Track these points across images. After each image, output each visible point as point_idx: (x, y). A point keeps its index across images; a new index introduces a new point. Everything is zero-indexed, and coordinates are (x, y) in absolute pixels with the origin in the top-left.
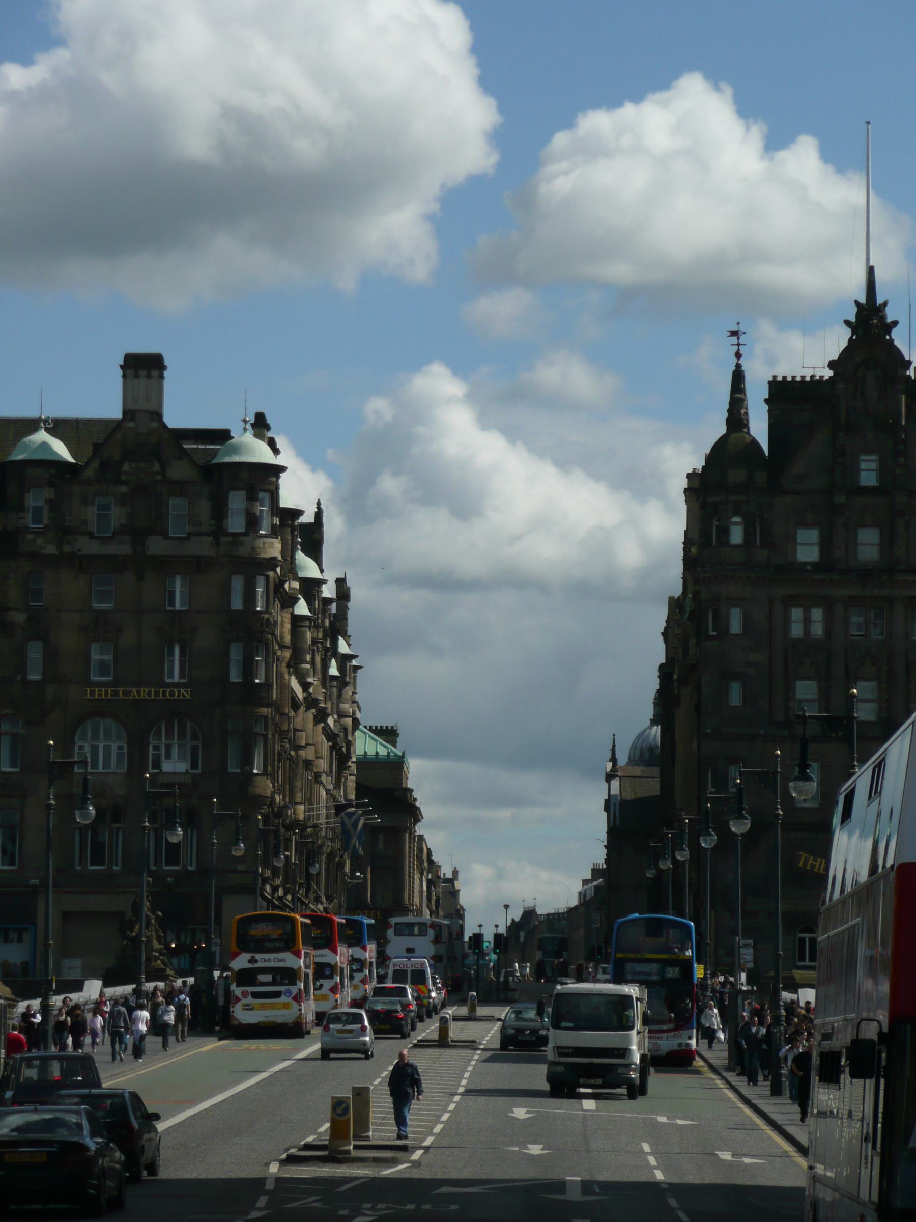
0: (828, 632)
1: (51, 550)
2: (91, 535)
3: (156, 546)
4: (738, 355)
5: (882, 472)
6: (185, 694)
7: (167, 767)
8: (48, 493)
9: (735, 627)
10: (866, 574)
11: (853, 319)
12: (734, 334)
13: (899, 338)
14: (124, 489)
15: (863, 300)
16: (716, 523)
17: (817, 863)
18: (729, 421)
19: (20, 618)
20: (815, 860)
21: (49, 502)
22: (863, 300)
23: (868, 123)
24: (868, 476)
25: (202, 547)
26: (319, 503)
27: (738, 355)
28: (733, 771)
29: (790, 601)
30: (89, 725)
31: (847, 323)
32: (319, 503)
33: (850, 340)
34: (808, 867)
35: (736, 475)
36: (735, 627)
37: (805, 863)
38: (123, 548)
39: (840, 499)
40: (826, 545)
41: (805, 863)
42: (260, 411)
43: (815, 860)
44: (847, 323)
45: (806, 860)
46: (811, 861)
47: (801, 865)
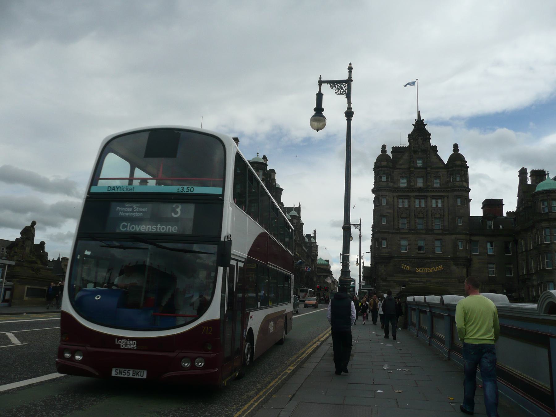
0: (409, 206)
5: (423, 163)
9: (384, 203)
10: (420, 190)
11: (415, 124)
15: (417, 119)
16: (378, 176)
17: (407, 267)
18: (382, 151)
20: (406, 266)
22: (417, 119)
23: (417, 79)
24: (420, 163)
26: (300, 203)
28: (384, 242)
29: (399, 197)
31: (413, 125)
32: (300, 203)
33: (414, 129)
34: (404, 268)
35: (384, 163)
36: (384, 203)
37: (404, 267)
39: (412, 169)
40: (408, 182)
41: (404, 267)
42: (264, 155)
43: (406, 266)
44: (413, 125)
45: (404, 266)
46: (405, 267)
47: (402, 268)
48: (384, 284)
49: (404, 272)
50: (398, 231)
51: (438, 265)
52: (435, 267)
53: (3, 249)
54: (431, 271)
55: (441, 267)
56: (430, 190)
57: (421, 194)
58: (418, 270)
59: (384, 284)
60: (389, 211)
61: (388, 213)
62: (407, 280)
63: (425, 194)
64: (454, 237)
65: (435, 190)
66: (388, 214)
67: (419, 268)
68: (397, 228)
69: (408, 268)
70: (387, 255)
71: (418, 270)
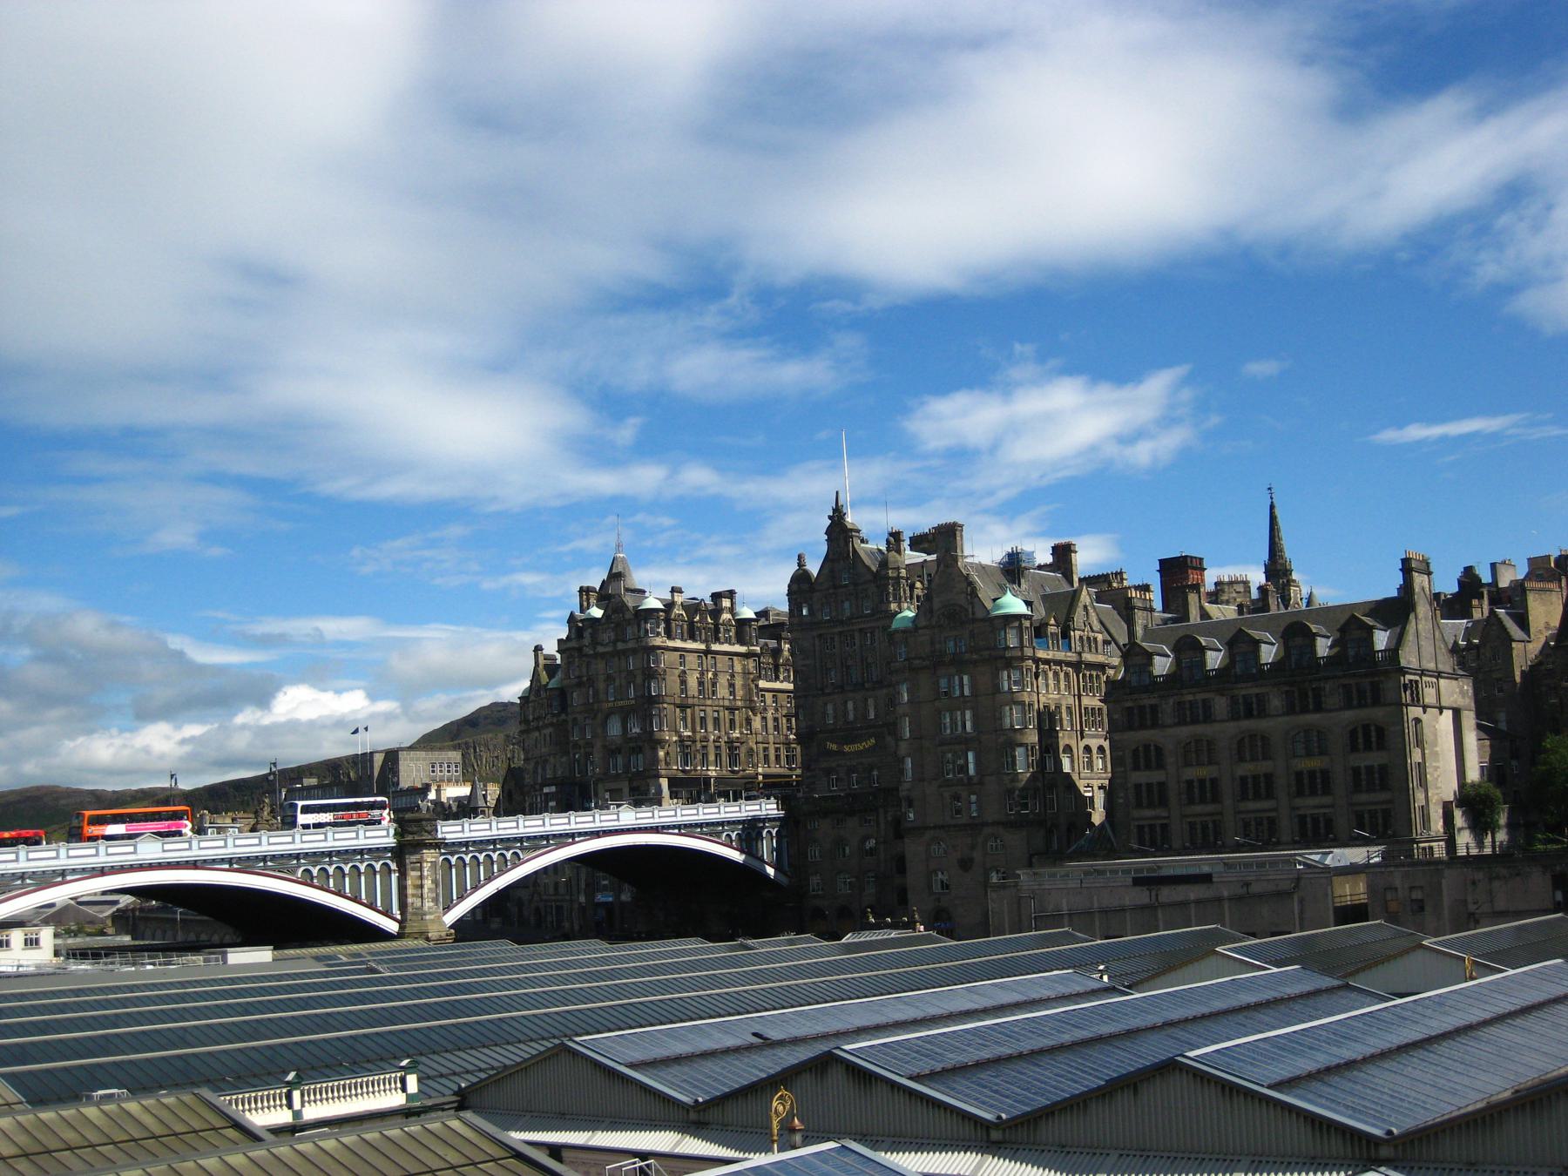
1: (592, 652)
2: (602, 645)
3: (620, 646)
4: (1272, 498)
6: (633, 702)
7: (634, 731)
8: (590, 630)
12: (1269, 489)
13: (850, 519)
14: (613, 625)
19: (585, 679)
21: (590, 634)
25: (631, 645)
27: (1272, 498)
30: (613, 716)
38: (609, 649)
48: (808, 774)
49: (830, 753)
50: (820, 692)
51: (870, 737)
52: (865, 740)
53: (433, 767)
54: (861, 748)
55: (873, 741)
56: (854, 621)
57: (846, 628)
58: (846, 749)
59: (808, 774)
60: (807, 662)
61: (803, 666)
62: (834, 765)
63: (851, 628)
64: (885, 691)
65: (859, 620)
66: (804, 668)
67: (847, 744)
68: (819, 686)
69: (834, 747)
70: (805, 730)
71: (846, 749)
